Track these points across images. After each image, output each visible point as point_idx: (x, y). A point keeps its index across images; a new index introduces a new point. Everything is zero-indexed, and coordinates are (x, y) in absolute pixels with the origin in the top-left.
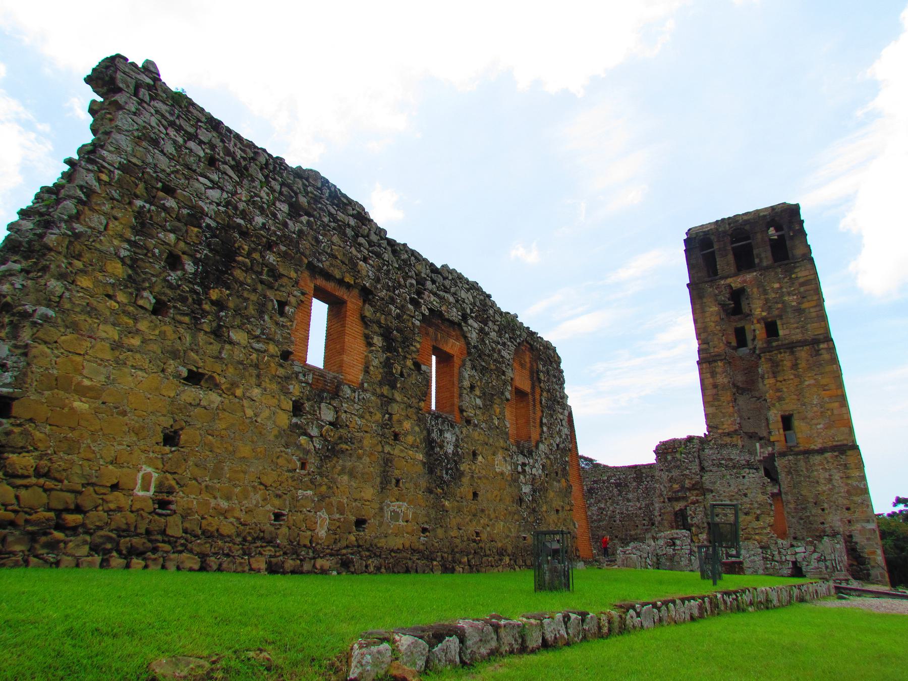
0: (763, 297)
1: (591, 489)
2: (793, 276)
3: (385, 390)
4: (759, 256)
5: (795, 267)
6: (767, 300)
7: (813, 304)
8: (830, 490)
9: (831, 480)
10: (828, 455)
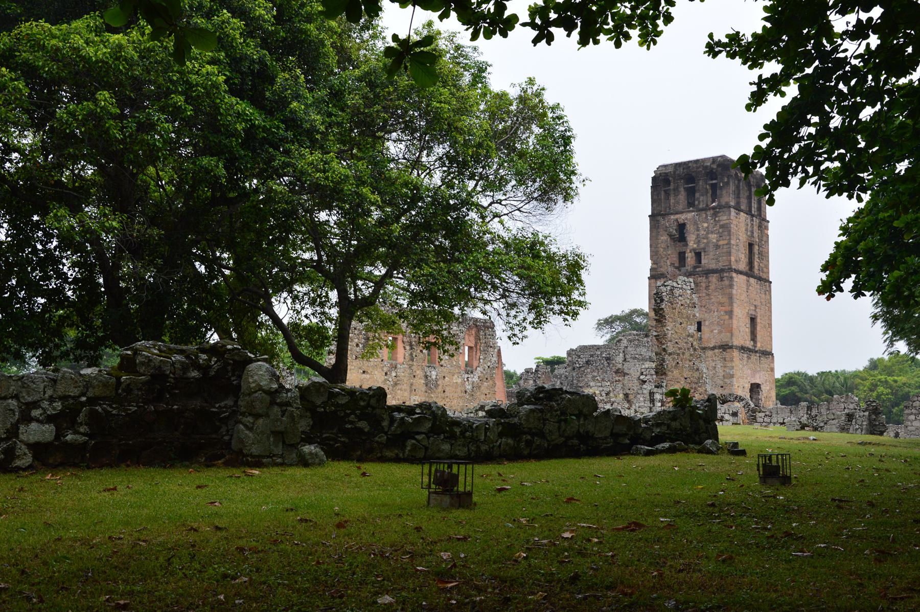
0: (696, 233)
1: (589, 361)
2: (717, 219)
3: (411, 363)
4: (698, 199)
5: (718, 212)
6: (698, 235)
7: (726, 242)
8: (714, 374)
9: (715, 368)
10: (716, 351)
